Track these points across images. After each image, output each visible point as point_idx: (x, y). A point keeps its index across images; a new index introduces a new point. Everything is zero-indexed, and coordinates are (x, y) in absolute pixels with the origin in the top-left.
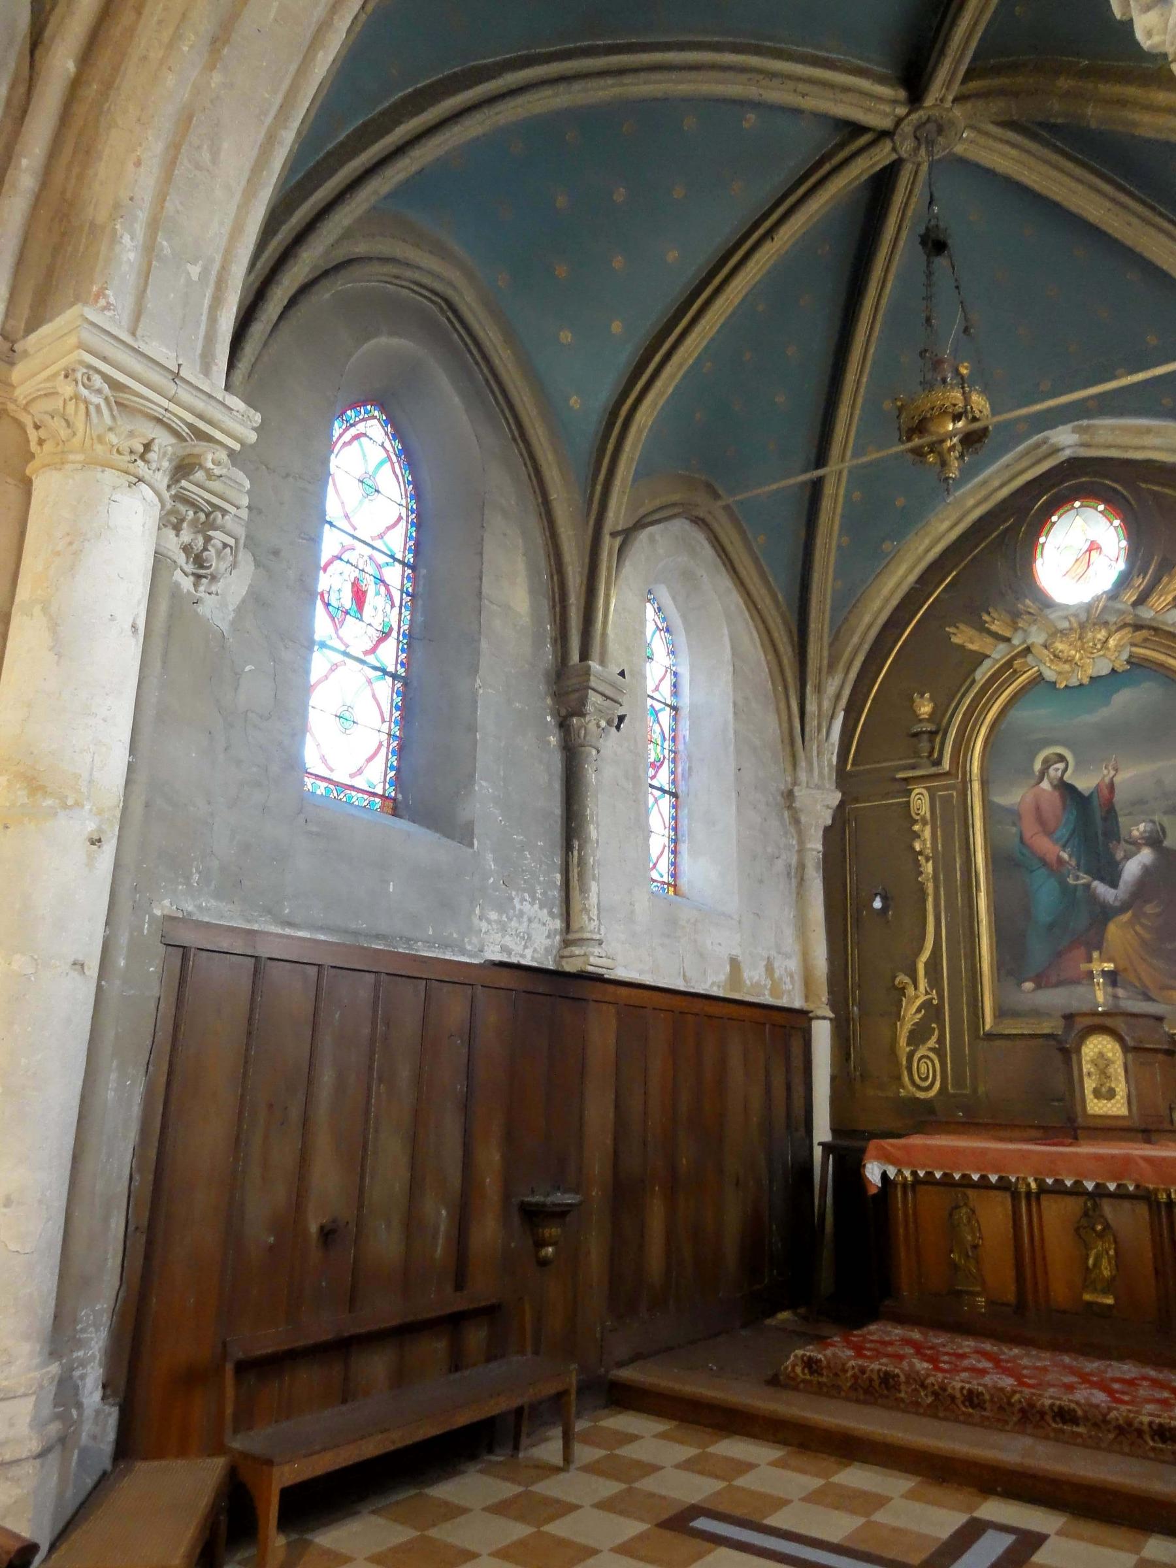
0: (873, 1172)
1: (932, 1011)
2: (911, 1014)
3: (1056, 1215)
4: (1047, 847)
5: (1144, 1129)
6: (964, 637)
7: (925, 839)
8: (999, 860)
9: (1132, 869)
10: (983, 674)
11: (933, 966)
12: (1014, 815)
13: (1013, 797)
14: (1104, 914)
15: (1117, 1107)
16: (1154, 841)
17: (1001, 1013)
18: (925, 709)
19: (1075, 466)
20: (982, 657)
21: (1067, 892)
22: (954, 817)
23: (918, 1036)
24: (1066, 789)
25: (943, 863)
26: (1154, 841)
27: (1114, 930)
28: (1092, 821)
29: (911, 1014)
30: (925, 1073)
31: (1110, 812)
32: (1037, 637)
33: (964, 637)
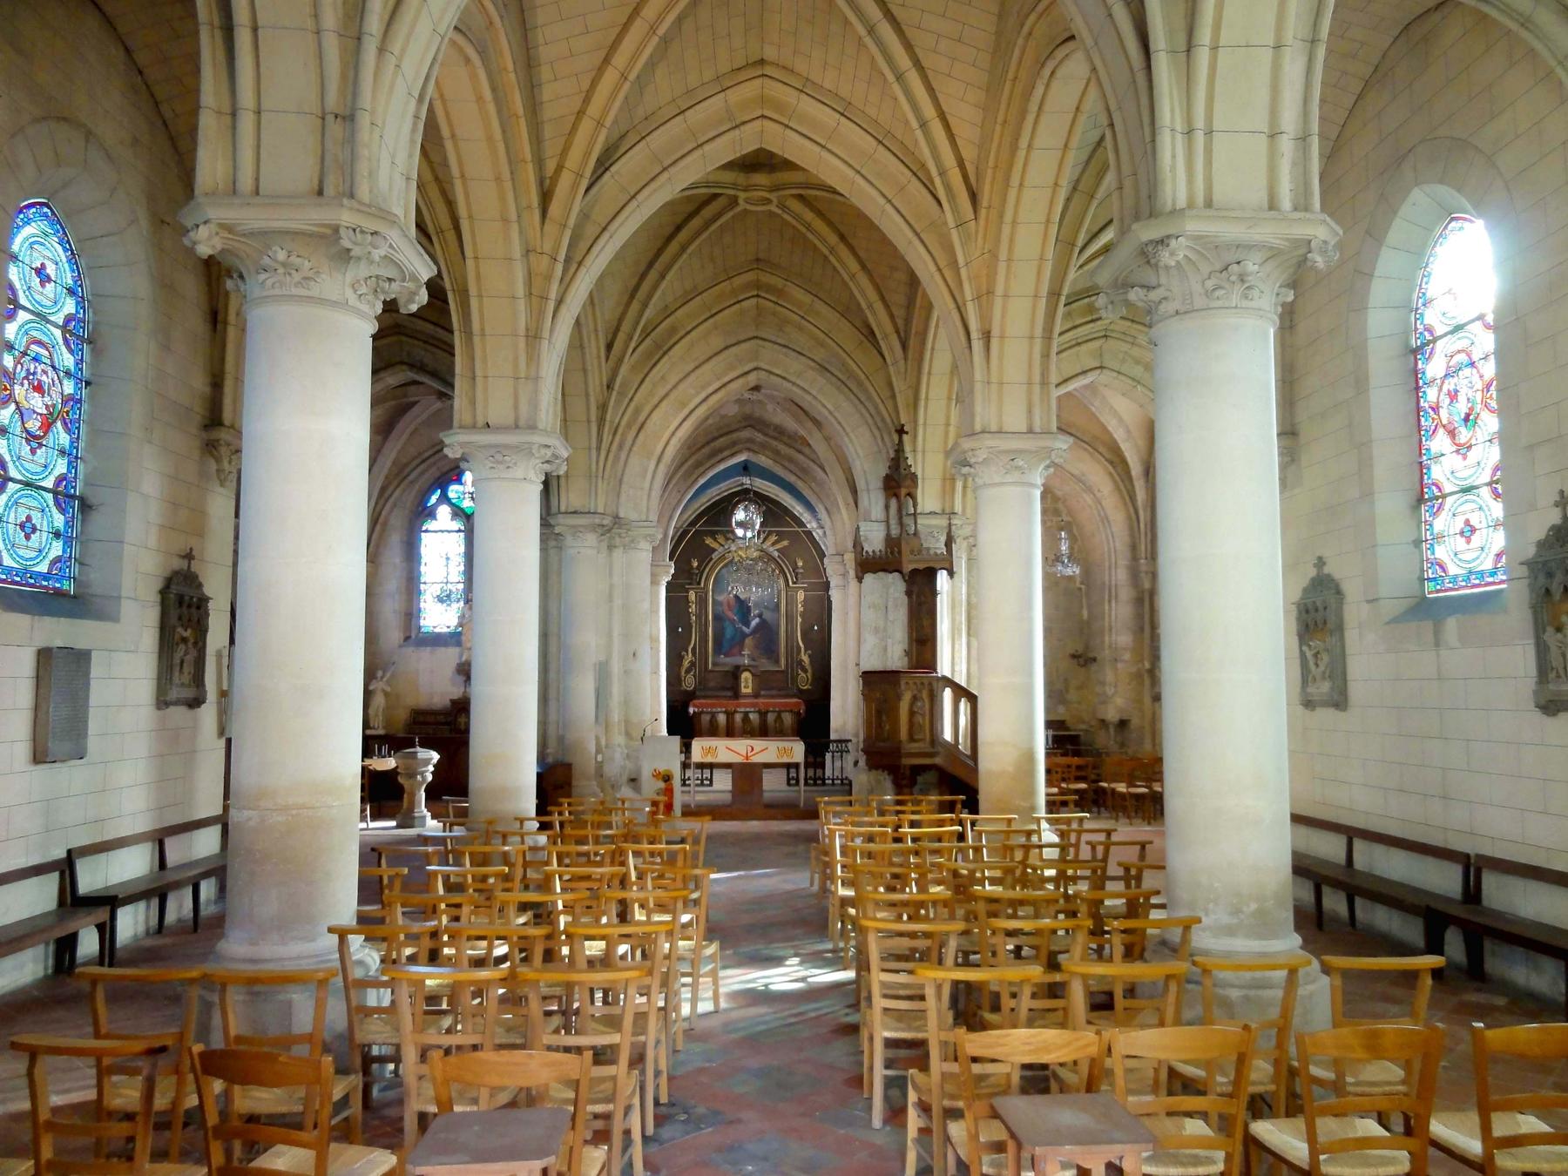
0: (691, 710)
1: (693, 664)
2: (686, 664)
3: (738, 718)
4: (730, 614)
5: (756, 695)
6: (709, 541)
7: (693, 609)
8: (717, 618)
9: (754, 623)
10: (715, 556)
11: (694, 649)
12: (721, 604)
13: (720, 598)
14: (745, 636)
15: (749, 690)
16: (760, 616)
17: (714, 664)
18: (695, 564)
19: (747, 491)
20: (714, 550)
21: (736, 629)
22: (702, 602)
23: (688, 671)
24: (736, 597)
25: (698, 617)
26: (760, 616)
27: (748, 641)
28: (742, 607)
29: (686, 664)
30: (689, 682)
31: (749, 609)
32: (733, 548)
33: (709, 541)
